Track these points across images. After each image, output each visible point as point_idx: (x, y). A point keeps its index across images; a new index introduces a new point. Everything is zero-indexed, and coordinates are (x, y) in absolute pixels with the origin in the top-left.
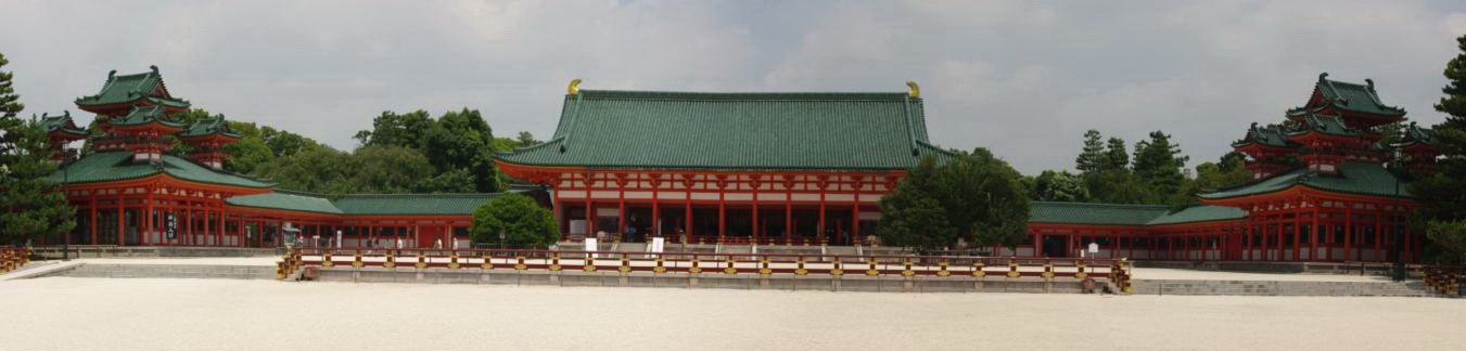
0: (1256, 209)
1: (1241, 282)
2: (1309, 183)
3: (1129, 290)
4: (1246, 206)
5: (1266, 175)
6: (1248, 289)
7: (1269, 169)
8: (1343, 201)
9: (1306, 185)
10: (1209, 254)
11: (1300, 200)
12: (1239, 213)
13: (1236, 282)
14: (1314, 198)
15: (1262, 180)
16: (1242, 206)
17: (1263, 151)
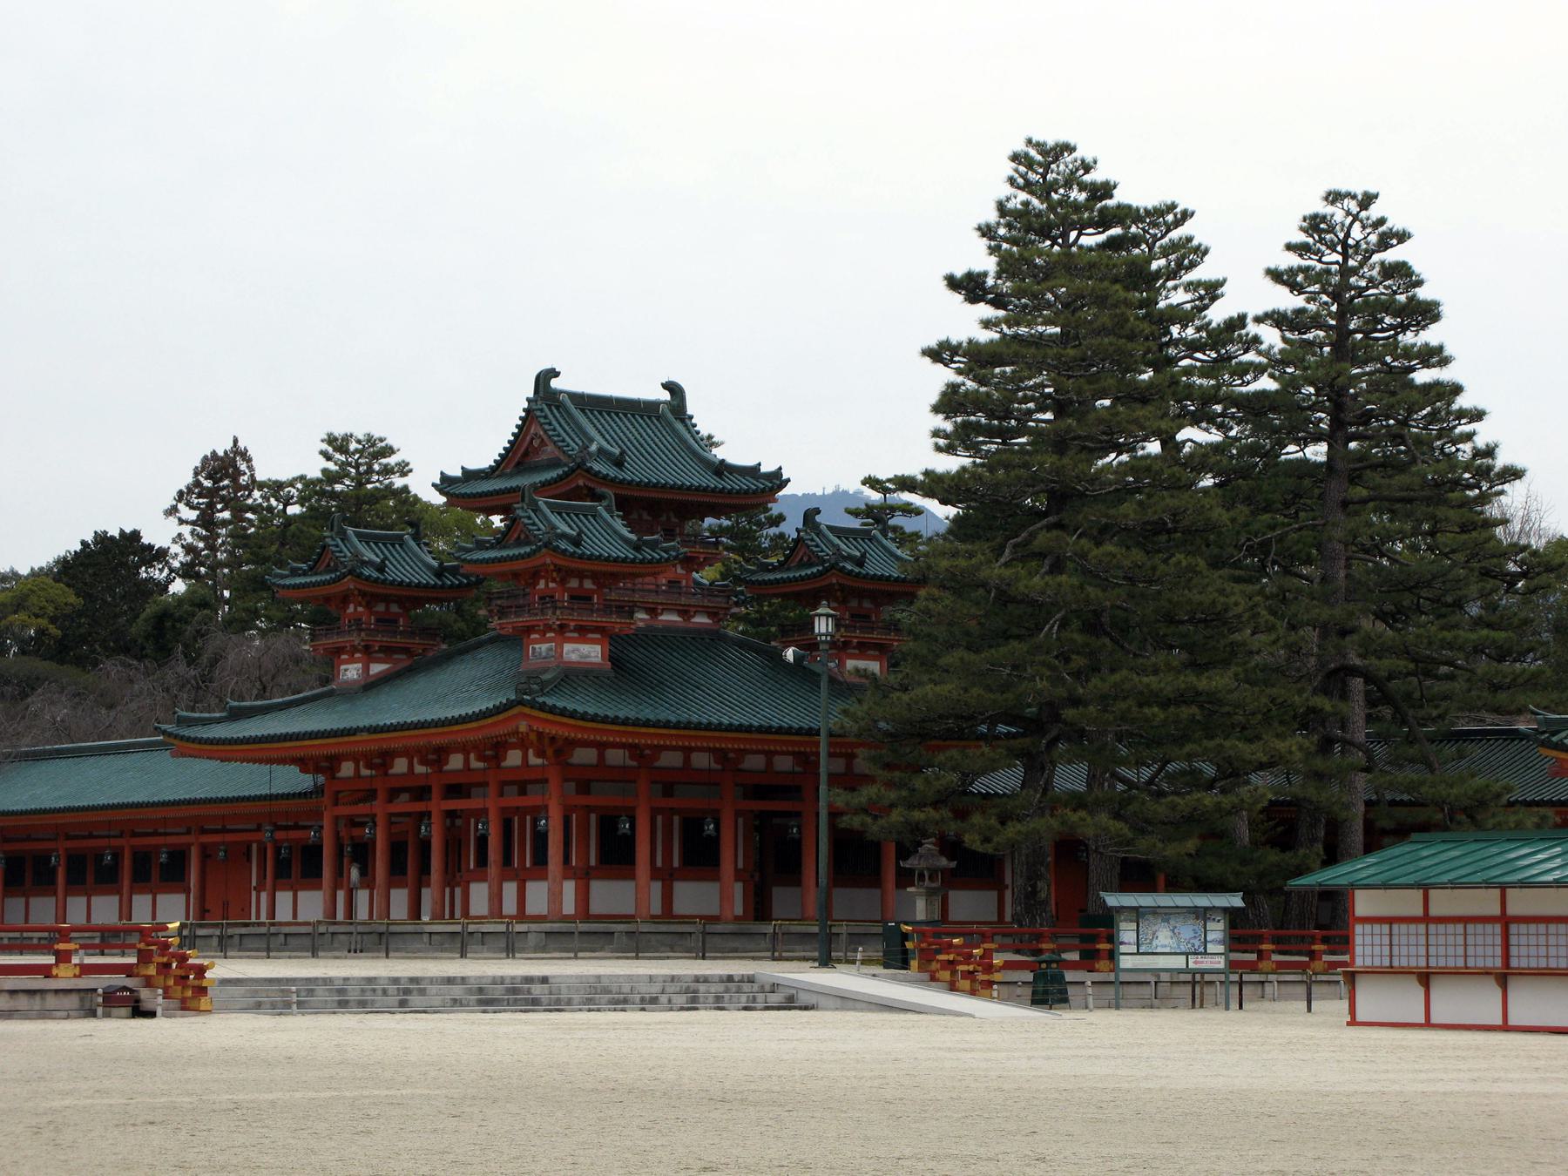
0: (347, 769)
1: (463, 980)
2: (550, 701)
3: (204, 1003)
4: (323, 764)
5: (377, 668)
6: (487, 998)
7: (388, 652)
8: (632, 748)
9: (543, 707)
10: (538, 896)
11: (498, 748)
12: (291, 779)
13: (450, 981)
14: (553, 739)
15: (370, 686)
16: (304, 764)
17: (370, 599)
